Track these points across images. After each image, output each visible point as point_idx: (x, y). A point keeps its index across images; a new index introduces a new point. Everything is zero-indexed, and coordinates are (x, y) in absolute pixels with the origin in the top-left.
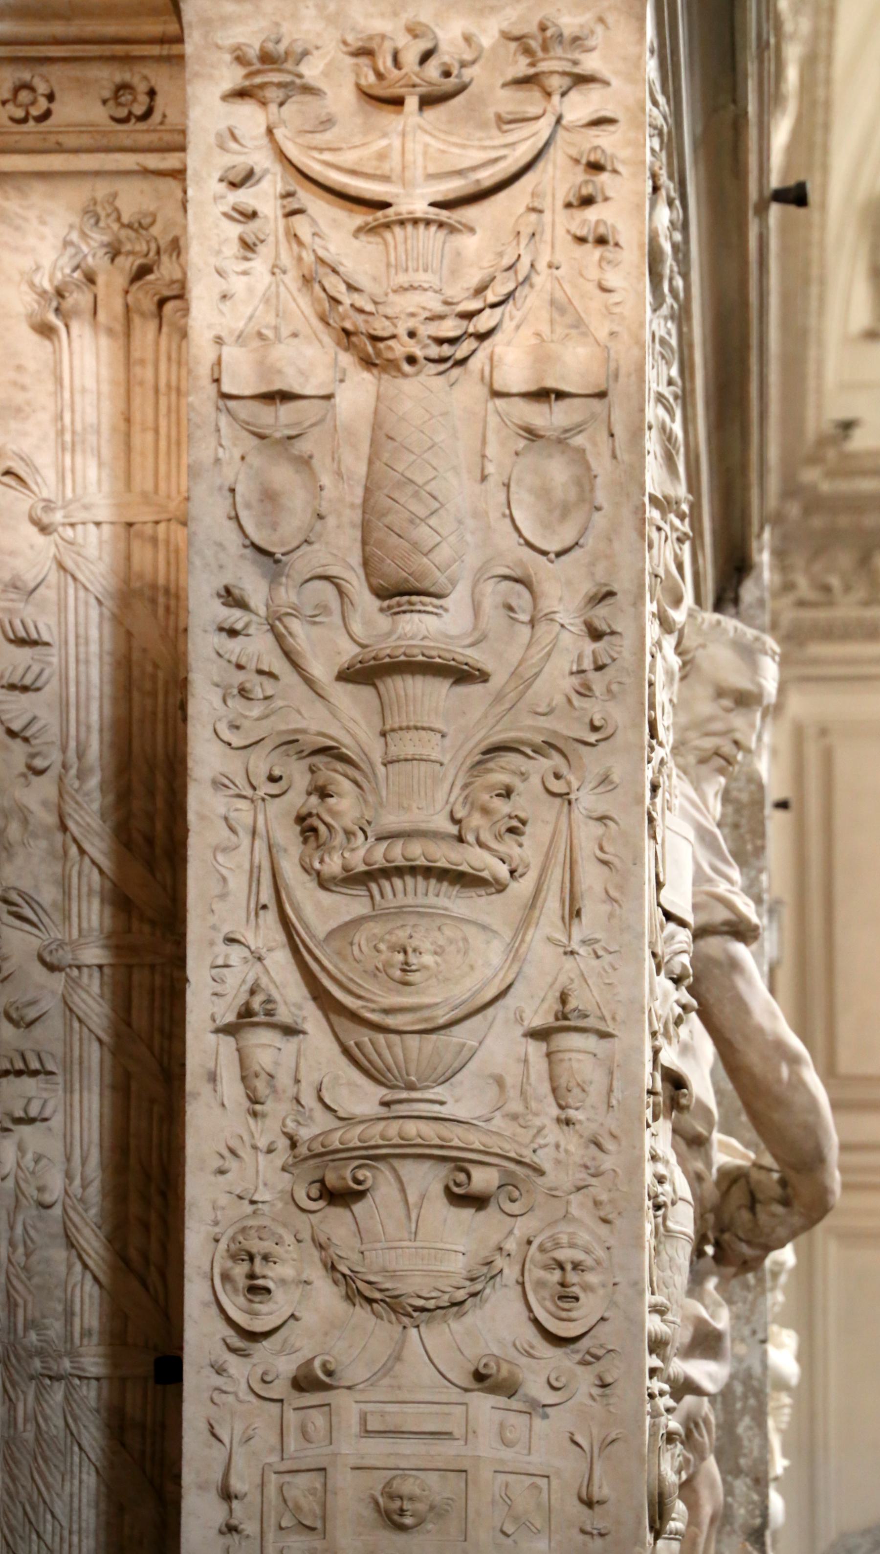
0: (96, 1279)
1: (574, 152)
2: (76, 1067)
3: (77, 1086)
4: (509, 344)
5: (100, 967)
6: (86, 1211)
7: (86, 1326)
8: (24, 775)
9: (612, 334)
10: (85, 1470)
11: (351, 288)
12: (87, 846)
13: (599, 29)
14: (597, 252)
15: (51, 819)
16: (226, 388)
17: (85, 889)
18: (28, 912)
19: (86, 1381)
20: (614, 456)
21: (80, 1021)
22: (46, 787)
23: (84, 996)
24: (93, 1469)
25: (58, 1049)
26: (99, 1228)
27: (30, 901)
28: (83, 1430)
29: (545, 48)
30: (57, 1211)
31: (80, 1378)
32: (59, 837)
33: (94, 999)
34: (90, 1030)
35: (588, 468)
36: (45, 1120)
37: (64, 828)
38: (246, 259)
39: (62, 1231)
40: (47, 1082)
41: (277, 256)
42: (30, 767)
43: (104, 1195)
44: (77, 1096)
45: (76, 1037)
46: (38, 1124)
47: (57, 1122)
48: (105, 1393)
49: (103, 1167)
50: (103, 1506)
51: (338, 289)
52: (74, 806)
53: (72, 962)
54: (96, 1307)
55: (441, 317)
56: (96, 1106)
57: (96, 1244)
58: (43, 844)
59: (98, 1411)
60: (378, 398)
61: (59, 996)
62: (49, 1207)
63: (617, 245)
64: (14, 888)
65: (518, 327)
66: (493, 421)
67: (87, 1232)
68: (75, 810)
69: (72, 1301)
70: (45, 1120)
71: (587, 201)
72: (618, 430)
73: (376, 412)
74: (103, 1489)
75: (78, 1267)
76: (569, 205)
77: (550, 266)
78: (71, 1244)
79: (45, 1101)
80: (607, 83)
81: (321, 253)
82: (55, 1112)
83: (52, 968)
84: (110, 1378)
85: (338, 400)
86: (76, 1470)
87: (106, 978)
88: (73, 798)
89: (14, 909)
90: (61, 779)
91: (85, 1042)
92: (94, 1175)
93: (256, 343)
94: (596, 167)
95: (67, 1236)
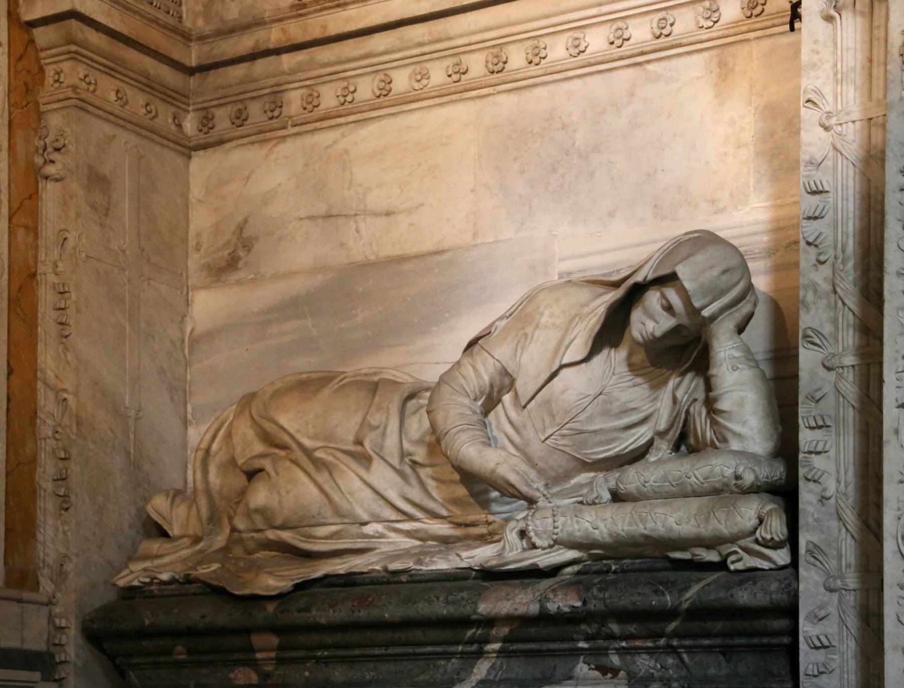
0: (853, 536)
2: (841, 422)
3: (842, 433)
5: (853, 366)
6: (847, 500)
7: (848, 562)
8: (815, 265)
10: (849, 639)
12: (846, 301)
15: (829, 288)
17: (845, 326)
18: (817, 341)
21: (843, 397)
22: (826, 270)
23: (846, 383)
25: (832, 412)
26: (854, 509)
27: (818, 333)
28: (848, 618)
30: (833, 501)
31: (846, 590)
32: (833, 296)
33: (849, 384)
34: (848, 402)
36: (826, 452)
37: (835, 292)
40: (827, 431)
42: (818, 261)
44: (842, 438)
45: (841, 405)
47: (832, 453)
48: (858, 597)
49: (856, 475)
52: (840, 279)
53: (839, 365)
56: (851, 443)
57: (853, 518)
58: (824, 302)
61: (833, 384)
62: (829, 499)
64: (810, 328)
67: (848, 511)
68: (840, 282)
69: (841, 549)
74: (858, 649)
75: (844, 530)
78: (840, 519)
79: (826, 442)
82: (831, 447)
83: (829, 369)
84: (861, 589)
86: (845, 639)
87: (856, 372)
88: (839, 275)
89: (810, 339)
90: (834, 265)
91: (846, 408)
92: (850, 481)
95: (838, 514)
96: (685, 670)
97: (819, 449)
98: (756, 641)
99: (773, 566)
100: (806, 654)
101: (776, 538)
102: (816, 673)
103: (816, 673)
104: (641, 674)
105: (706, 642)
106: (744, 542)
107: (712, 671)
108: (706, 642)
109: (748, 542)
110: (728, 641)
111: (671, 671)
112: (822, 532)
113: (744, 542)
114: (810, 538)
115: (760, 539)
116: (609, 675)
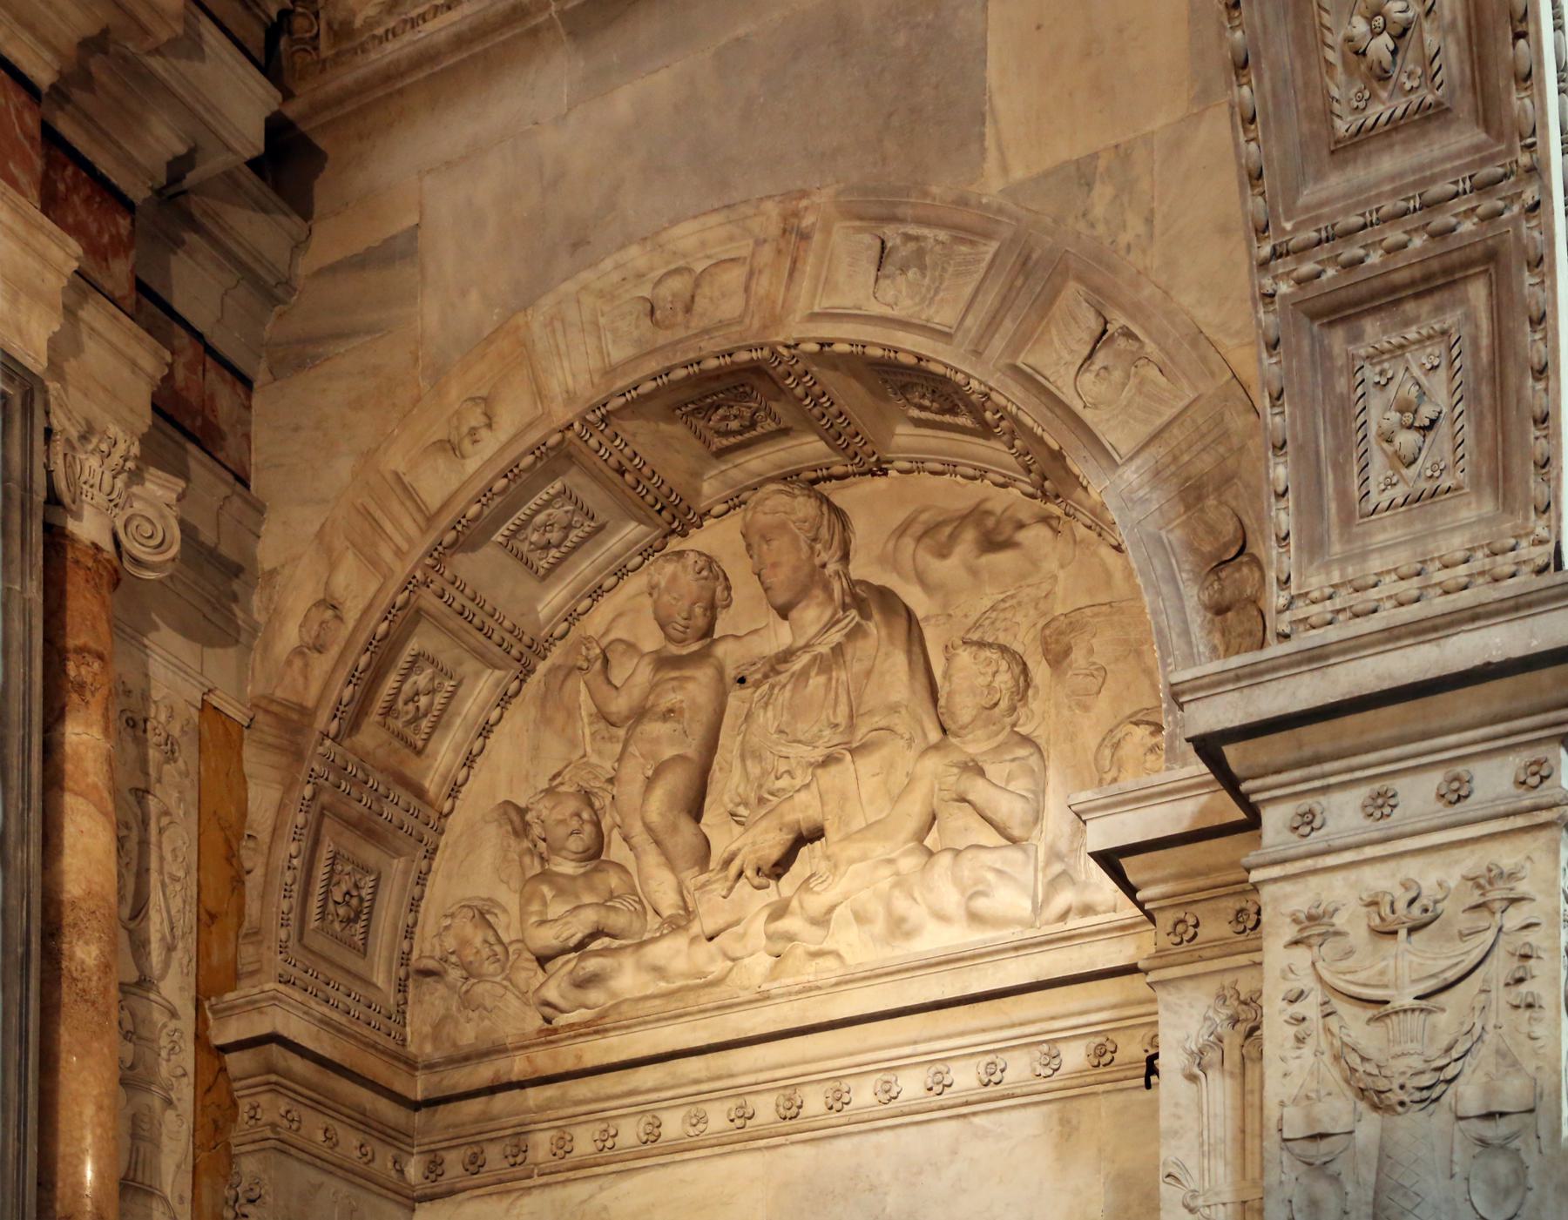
1: (1511, 948)
4: (1468, 1083)
9: (1538, 1068)
11: (1363, 1059)
13: (1528, 865)
14: (1528, 1013)
16: (1286, 1135)
20: (1540, 1152)
29: (1490, 882)
35: (1522, 1162)
38: (1299, 1048)
41: (1319, 1044)
51: (1354, 1060)
55: (1423, 1072)
60: (1383, 1130)
63: (1540, 1007)
65: (1474, 1071)
66: (1458, 1136)
71: (1520, 980)
72: (1542, 1133)
73: (1381, 1138)
76: (1507, 985)
77: (1495, 1027)
80: (1533, 900)
81: (1346, 1039)
85: (1356, 1134)
93: (1305, 1103)
94: (1526, 957)
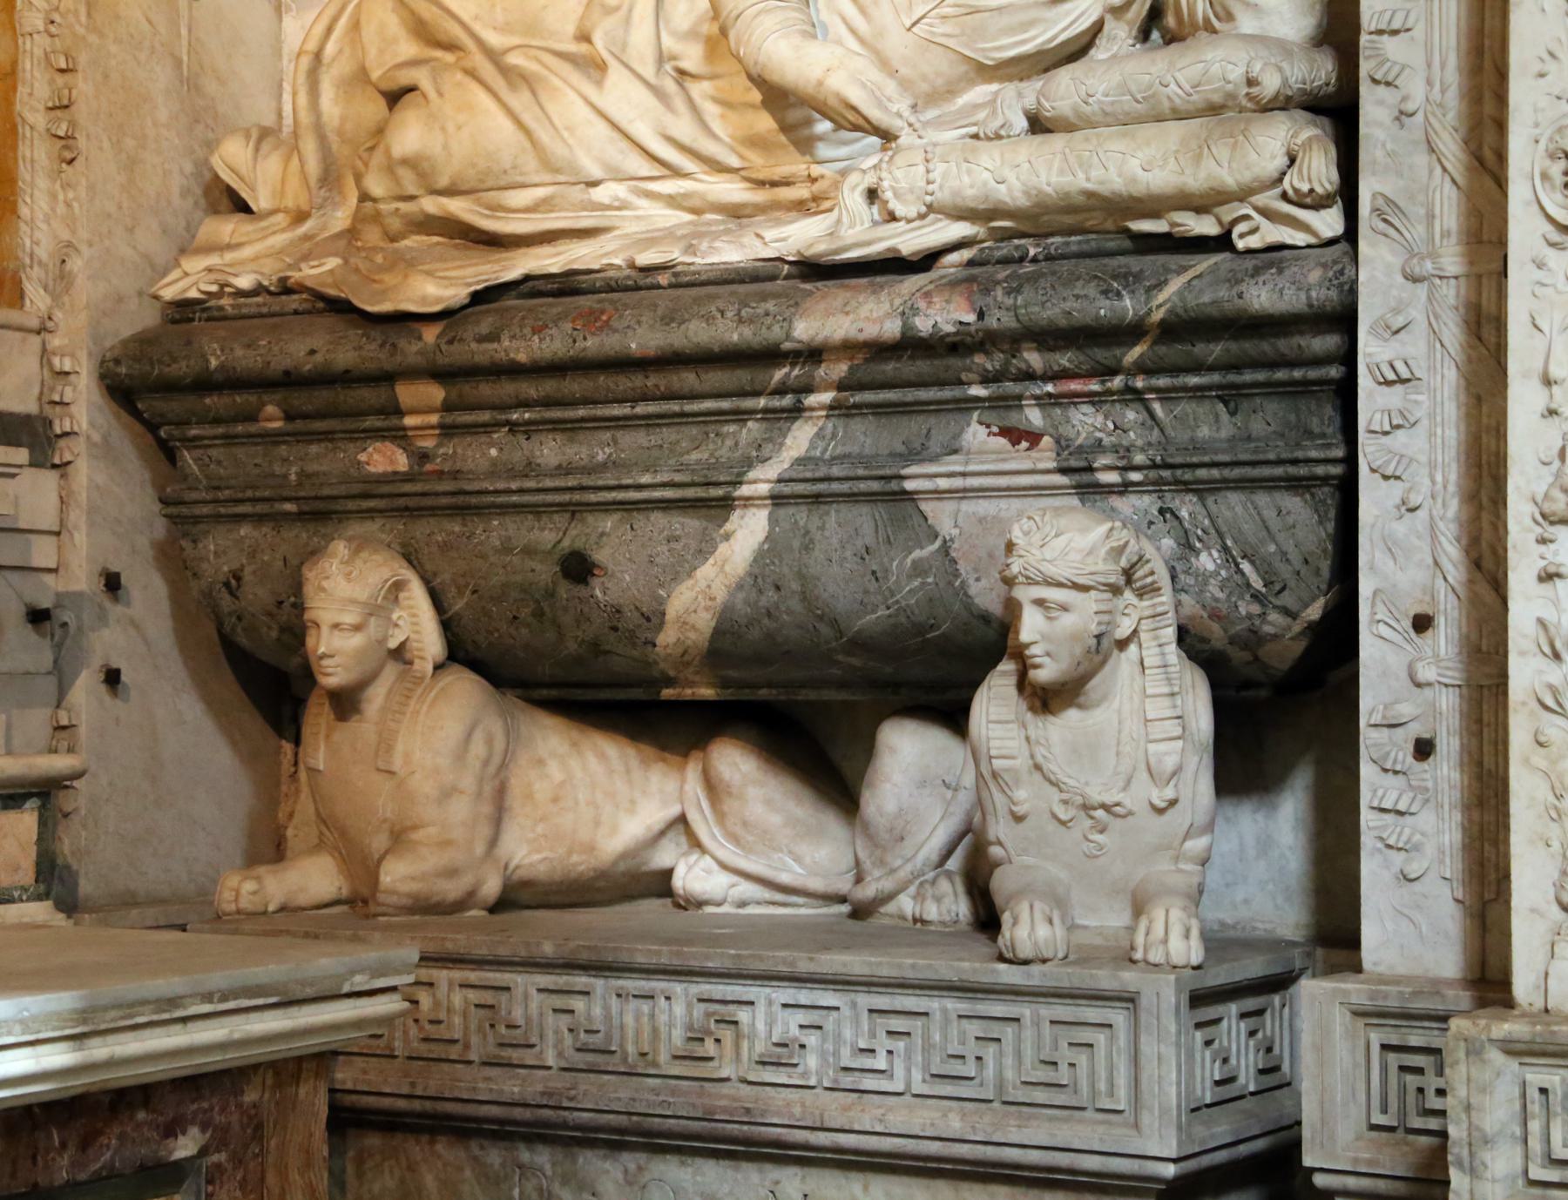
0: (1454, 181)
6: (1444, 115)
7: (1445, 227)
10: (1446, 365)
19: (1445, 281)
24: (1453, 363)
26: (1456, 131)
30: (1419, 117)
31: (1441, 278)
36: (1408, 30)
39: (1424, 138)
43: (1462, 97)
46: (1402, 34)
47: (1419, 32)
48: (1463, 291)
49: (1460, 69)
50: (1463, 398)
54: (1454, 210)
59: (1457, 309)
67: (1446, 136)
69: (1433, 204)
70: (1408, 30)
74: (1462, 382)
75: (1438, 170)
82: (1417, 21)
86: (1439, 366)
95: (1429, 142)
96: (1156, 431)
97: (1396, 25)
98: (1281, 375)
99: (1313, 241)
100: (1370, 395)
101: (1319, 190)
102: (1387, 428)
103: (1387, 428)
104: (1079, 442)
105: (1194, 380)
106: (1261, 199)
107: (1204, 432)
108: (1194, 380)
109: (1269, 199)
110: (1233, 378)
111: (1132, 434)
112: (1399, 174)
113: (1261, 199)
114: (1379, 188)
115: (1290, 192)
116: (1024, 444)
